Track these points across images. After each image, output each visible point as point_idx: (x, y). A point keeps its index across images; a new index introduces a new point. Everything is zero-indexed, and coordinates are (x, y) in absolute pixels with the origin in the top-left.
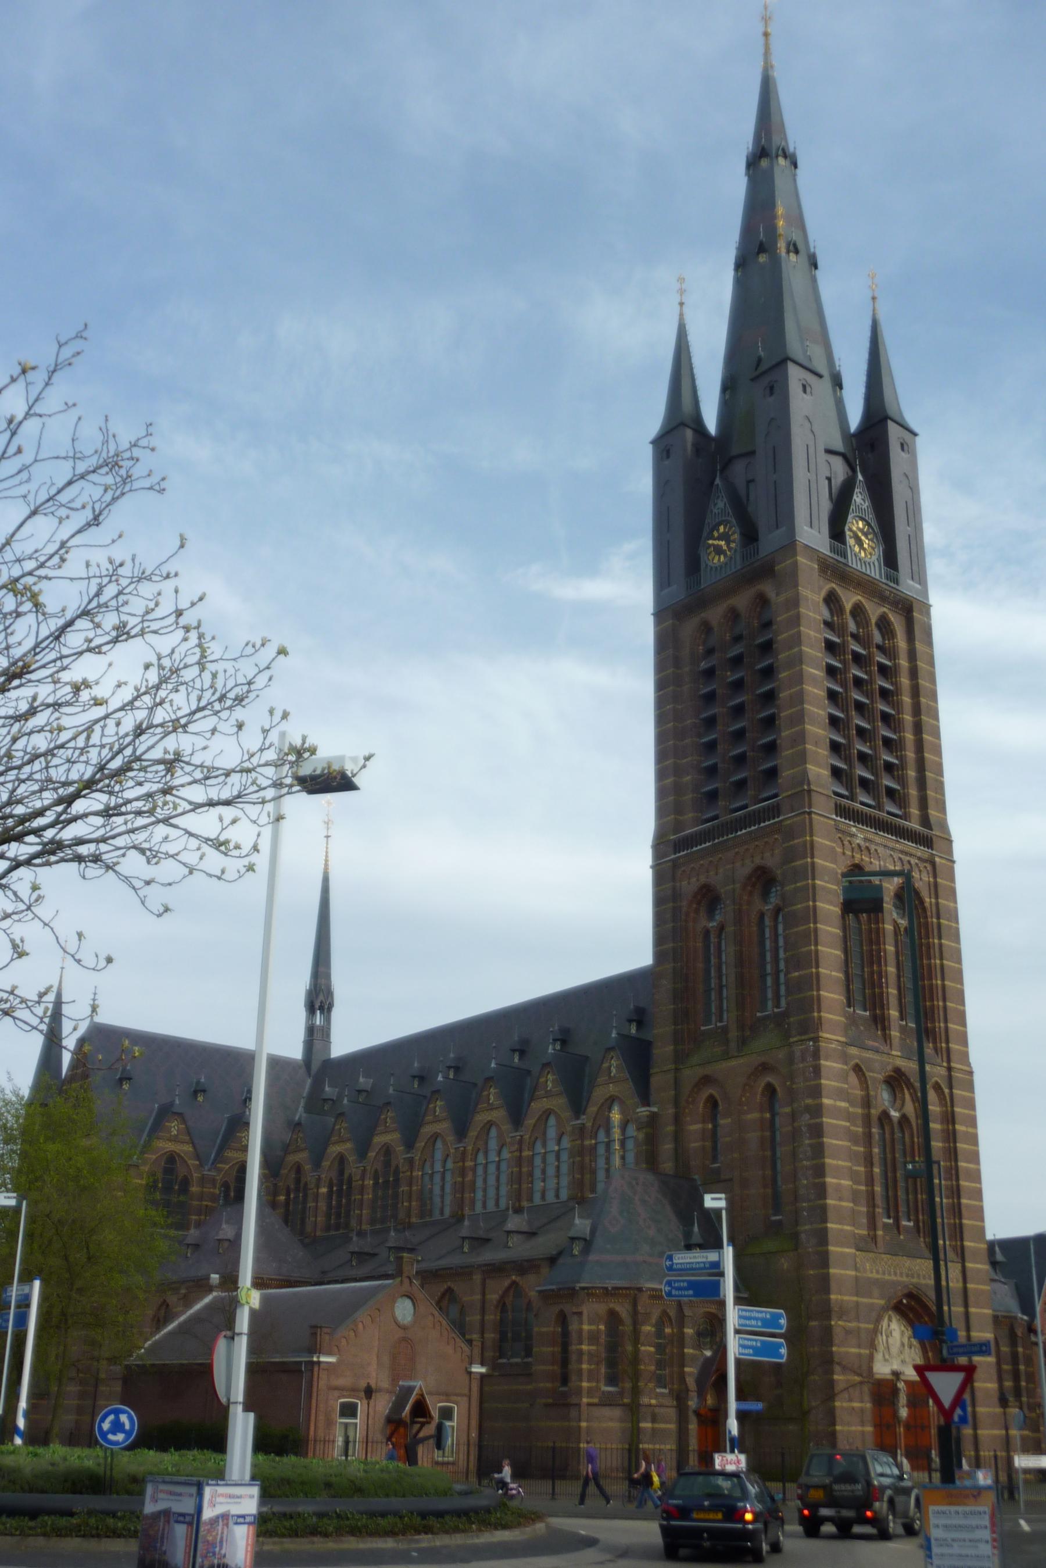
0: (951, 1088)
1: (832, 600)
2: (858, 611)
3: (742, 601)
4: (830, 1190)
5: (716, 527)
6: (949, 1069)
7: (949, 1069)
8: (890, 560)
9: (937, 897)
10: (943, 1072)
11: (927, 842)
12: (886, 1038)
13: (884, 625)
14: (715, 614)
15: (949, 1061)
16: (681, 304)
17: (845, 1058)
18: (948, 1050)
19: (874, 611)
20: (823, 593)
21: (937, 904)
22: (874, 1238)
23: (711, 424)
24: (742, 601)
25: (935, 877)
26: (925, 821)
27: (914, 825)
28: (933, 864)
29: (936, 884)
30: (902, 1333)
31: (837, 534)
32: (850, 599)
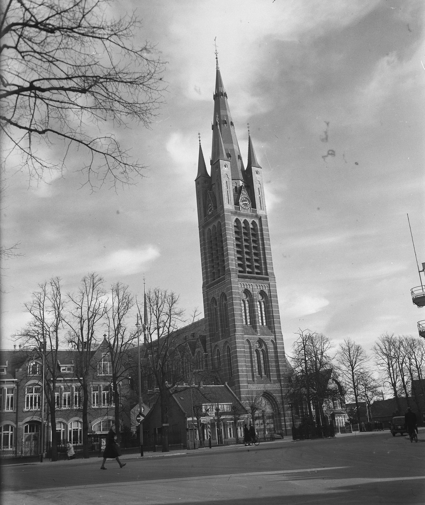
0: (276, 340)
1: (237, 221)
2: (245, 222)
3: (216, 224)
4: (240, 371)
5: (209, 205)
6: (275, 336)
7: (275, 336)
8: (254, 206)
9: (270, 293)
10: (274, 337)
11: (267, 279)
12: (256, 331)
13: (253, 223)
14: (211, 227)
15: (275, 334)
16: (200, 140)
17: (243, 338)
18: (275, 331)
19: (250, 221)
20: (234, 220)
21: (270, 294)
22: (254, 380)
23: (209, 173)
24: (216, 224)
25: (270, 288)
26: (267, 274)
27: (264, 276)
28: (269, 284)
29: (270, 289)
30: (265, 402)
31: (237, 203)
32: (242, 219)
